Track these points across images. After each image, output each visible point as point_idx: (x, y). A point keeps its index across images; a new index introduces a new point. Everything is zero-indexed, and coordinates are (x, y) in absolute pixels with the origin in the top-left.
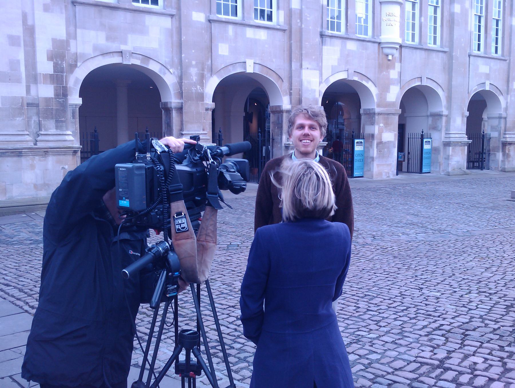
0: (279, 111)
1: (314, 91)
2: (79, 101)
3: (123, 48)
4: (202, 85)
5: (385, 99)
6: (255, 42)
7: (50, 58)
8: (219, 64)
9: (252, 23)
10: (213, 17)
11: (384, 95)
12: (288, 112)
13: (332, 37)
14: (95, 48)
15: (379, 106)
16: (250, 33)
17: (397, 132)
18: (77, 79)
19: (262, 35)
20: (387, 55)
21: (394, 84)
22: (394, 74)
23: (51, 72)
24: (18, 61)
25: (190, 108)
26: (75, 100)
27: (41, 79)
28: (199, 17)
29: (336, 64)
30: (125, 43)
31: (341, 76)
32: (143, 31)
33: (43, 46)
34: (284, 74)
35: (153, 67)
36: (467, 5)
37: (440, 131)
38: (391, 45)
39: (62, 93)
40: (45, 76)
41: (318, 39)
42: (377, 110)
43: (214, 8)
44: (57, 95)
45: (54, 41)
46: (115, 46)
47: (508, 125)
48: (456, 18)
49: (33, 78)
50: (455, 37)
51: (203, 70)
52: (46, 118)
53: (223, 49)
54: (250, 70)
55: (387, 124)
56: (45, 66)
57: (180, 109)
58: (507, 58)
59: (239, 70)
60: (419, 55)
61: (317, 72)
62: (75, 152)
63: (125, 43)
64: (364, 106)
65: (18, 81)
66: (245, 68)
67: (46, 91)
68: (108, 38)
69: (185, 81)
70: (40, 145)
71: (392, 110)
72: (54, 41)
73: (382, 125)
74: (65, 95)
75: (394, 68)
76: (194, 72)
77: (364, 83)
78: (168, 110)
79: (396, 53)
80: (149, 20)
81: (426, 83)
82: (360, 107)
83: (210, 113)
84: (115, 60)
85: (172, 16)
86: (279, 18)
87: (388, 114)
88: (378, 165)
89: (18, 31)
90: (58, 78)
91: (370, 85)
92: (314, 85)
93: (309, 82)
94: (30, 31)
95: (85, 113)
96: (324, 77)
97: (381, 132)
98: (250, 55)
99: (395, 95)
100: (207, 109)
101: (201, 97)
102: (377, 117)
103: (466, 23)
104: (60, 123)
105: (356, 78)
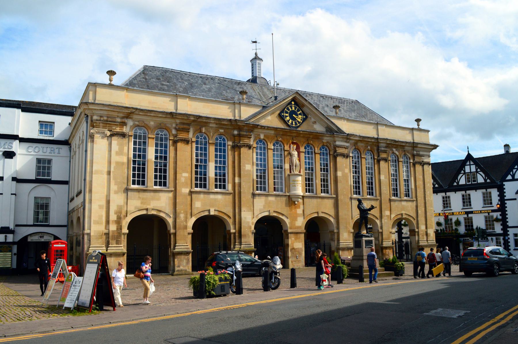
0: (230, 234)
1: (249, 222)
2: (127, 231)
3: (148, 207)
4: (186, 221)
5: (295, 225)
6: (216, 200)
7: (116, 213)
8: (195, 211)
9: (213, 191)
10: (192, 190)
11: (296, 222)
12: (235, 233)
13: (259, 195)
14: (136, 208)
15: (291, 228)
16: (212, 196)
17: (304, 243)
18: (127, 222)
19: (219, 197)
20: (295, 202)
21: (299, 216)
22: (300, 211)
23: (115, 219)
24: (102, 216)
25: (180, 234)
26: (125, 230)
27: (111, 222)
28: (186, 190)
29: (262, 208)
30: (150, 205)
31: (266, 214)
32: (159, 199)
33: (113, 208)
34: (231, 215)
35: (162, 215)
36: (347, 171)
37: (334, 241)
38: (297, 196)
39: (120, 228)
40: (113, 221)
41: (250, 196)
42: (289, 231)
43: (194, 185)
44: (117, 229)
45: (118, 206)
46: (145, 207)
47: (384, 236)
48: (339, 179)
49: (108, 222)
50: (339, 189)
51: (187, 215)
52: (112, 239)
53: (198, 205)
54: (212, 213)
55: (296, 239)
56: (113, 217)
57: (175, 234)
58: (379, 198)
59: (206, 213)
60: (315, 201)
61: (251, 213)
62: (124, 254)
63: (150, 205)
64: (284, 228)
65: (102, 224)
66: (209, 212)
67: (113, 227)
68: (141, 203)
69: (177, 221)
70: (109, 251)
71: (299, 231)
72: (118, 206)
73: (293, 239)
74: (121, 229)
75: (299, 208)
76: (182, 216)
77: (281, 216)
78: (170, 235)
79: (300, 201)
80: (161, 194)
81: (321, 215)
82: (282, 229)
83: (190, 236)
84: (144, 212)
85: (172, 191)
86: (230, 187)
87: (297, 233)
88: (292, 262)
89: (104, 203)
90: (118, 222)
91: (283, 218)
92: (249, 220)
93: (245, 218)
94: (108, 202)
95: (129, 236)
96: (255, 215)
97: (292, 244)
98: (212, 206)
99: (301, 223)
100: (189, 234)
101: (186, 227)
102: (289, 235)
103: (347, 181)
104: (118, 242)
105: (275, 214)
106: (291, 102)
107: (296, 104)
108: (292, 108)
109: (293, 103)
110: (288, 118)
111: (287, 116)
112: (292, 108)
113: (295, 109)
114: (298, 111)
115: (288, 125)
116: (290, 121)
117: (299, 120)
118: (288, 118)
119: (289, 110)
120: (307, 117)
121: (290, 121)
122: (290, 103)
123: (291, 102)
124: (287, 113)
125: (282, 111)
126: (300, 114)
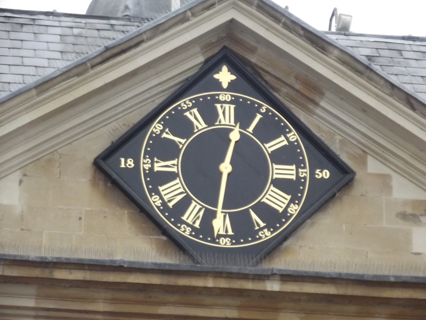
106: (211, 66)
107: (251, 79)
108: (210, 116)
109: (225, 76)
110: (173, 191)
111: (172, 176)
112: (210, 116)
113: (243, 116)
114: (269, 130)
115: (176, 243)
116: (193, 214)
117: (275, 198)
118: (173, 191)
119: (183, 127)
120: (344, 176)
121: (193, 214)
122: (200, 80)
123: (211, 66)
124: (165, 150)
125: (127, 141)
126: (283, 156)
